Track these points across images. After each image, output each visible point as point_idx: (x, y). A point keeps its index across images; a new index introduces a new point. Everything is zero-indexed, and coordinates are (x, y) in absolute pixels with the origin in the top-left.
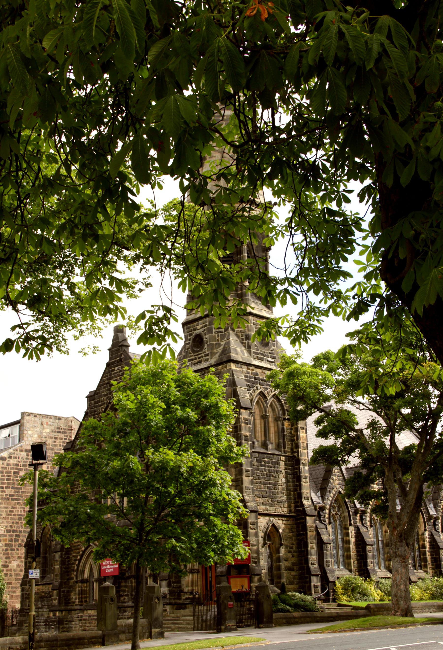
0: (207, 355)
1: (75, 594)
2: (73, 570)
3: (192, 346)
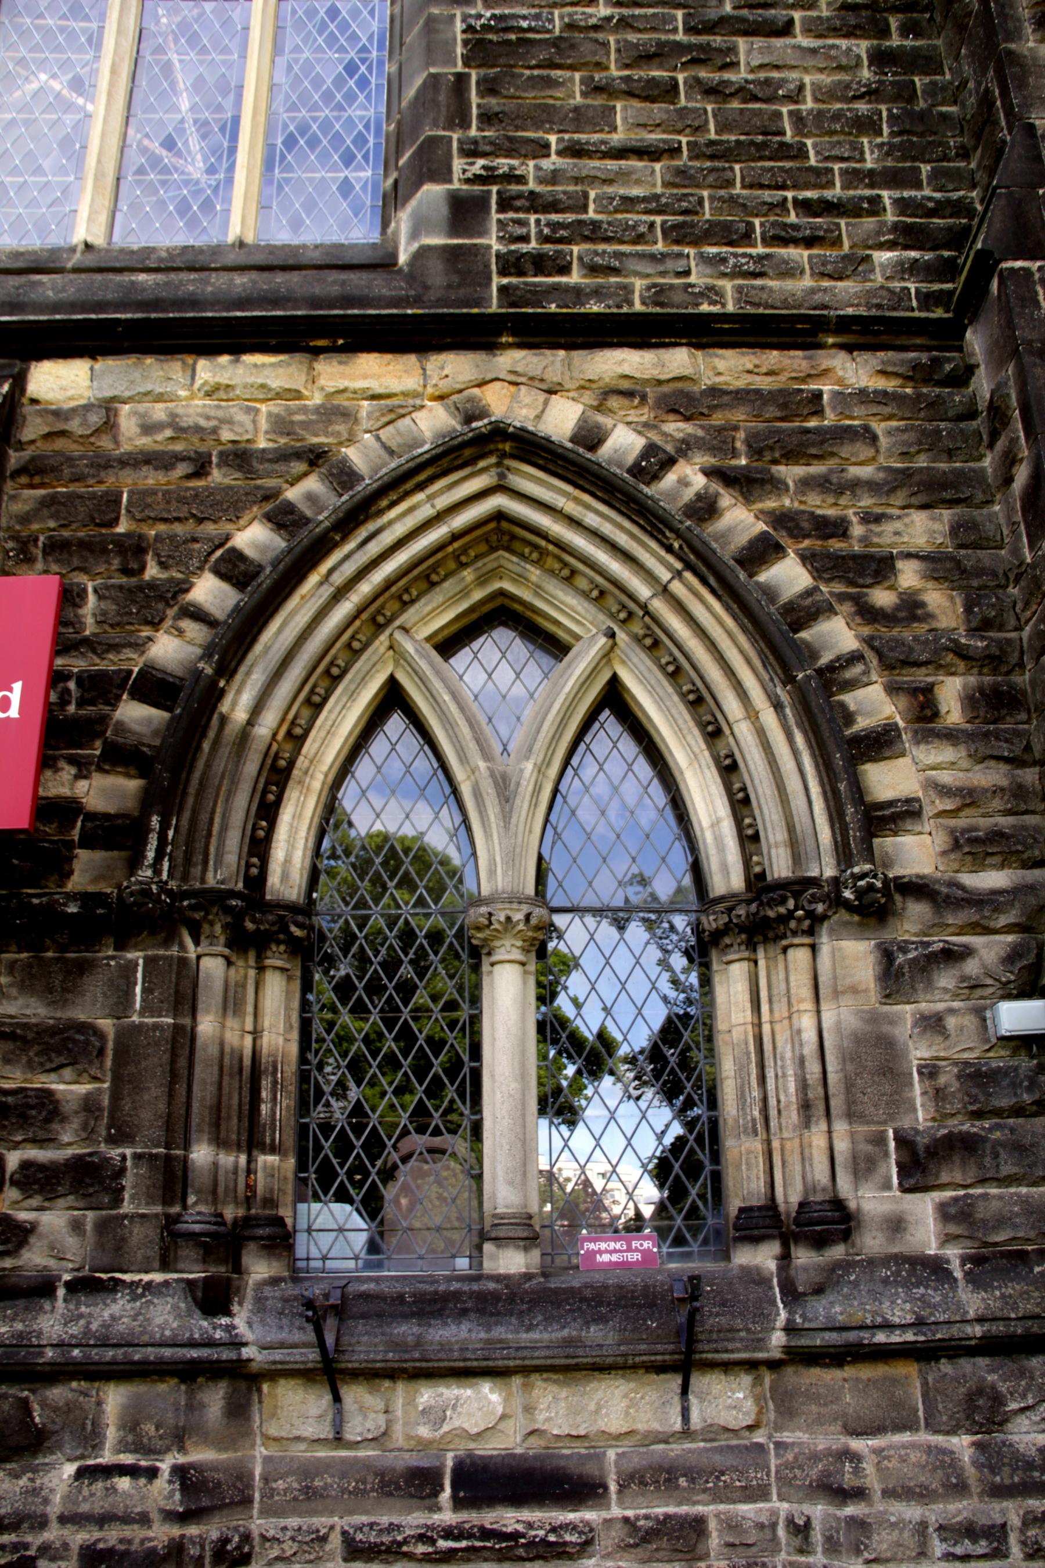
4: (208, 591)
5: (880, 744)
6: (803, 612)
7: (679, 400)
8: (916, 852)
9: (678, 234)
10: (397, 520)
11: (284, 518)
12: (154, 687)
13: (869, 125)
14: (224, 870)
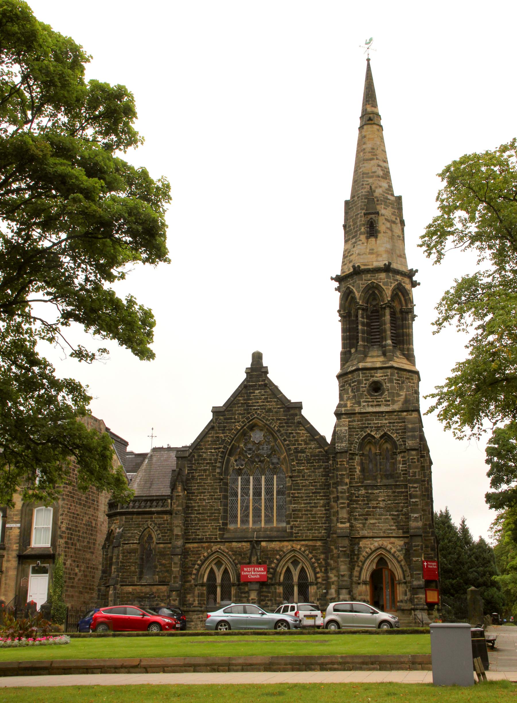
0: (386, 401)
1: (193, 597)
2: (191, 574)
3: (368, 390)
4: (275, 561)
5: (318, 573)
6: (314, 563)
7: (307, 546)
8: (320, 580)
9: (308, 530)
10: (288, 556)
11: (280, 555)
12: (272, 568)
13: (323, 517)
14: (277, 581)
